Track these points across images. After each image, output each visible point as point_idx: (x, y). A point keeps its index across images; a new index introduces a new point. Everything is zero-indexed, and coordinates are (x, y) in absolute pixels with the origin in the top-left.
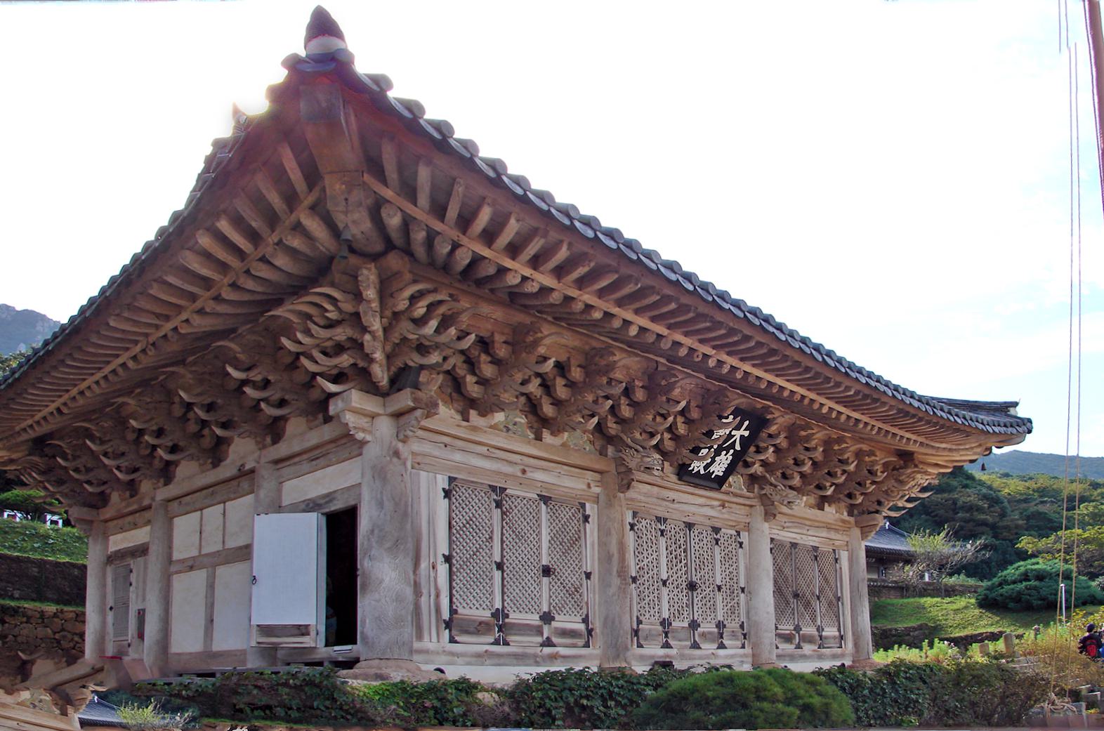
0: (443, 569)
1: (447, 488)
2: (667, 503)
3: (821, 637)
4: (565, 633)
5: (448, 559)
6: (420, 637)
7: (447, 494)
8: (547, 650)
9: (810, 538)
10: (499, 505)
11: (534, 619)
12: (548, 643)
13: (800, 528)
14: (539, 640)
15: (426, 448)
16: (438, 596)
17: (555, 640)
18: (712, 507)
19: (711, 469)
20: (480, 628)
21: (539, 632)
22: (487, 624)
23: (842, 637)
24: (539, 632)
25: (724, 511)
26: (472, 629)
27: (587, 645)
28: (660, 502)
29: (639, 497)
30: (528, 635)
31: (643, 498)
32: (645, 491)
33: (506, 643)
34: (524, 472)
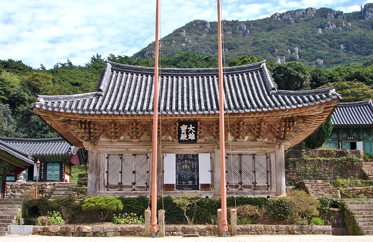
0: (106, 174)
1: (107, 156)
2: (177, 150)
3: (255, 186)
4: (139, 187)
5: (107, 172)
6: (99, 190)
7: (107, 158)
8: (134, 192)
9: (250, 151)
10: (121, 158)
11: (130, 184)
12: (134, 190)
13: (243, 149)
14: (132, 189)
15: (101, 149)
16: (104, 181)
17: (136, 189)
18: (196, 148)
19: (190, 138)
20: (115, 187)
21: (132, 187)
22: (117, 186)
23: (268, 186)
24: (132, 187)
25: (202, 148)
26: (113, 187)
27: (146, 190)
28: (174, 150)
29: (166, 150)
30: (130, 188)
31: (167, 150)
32: (168, 148)
33: (122, 190)
34: (128, 149)
